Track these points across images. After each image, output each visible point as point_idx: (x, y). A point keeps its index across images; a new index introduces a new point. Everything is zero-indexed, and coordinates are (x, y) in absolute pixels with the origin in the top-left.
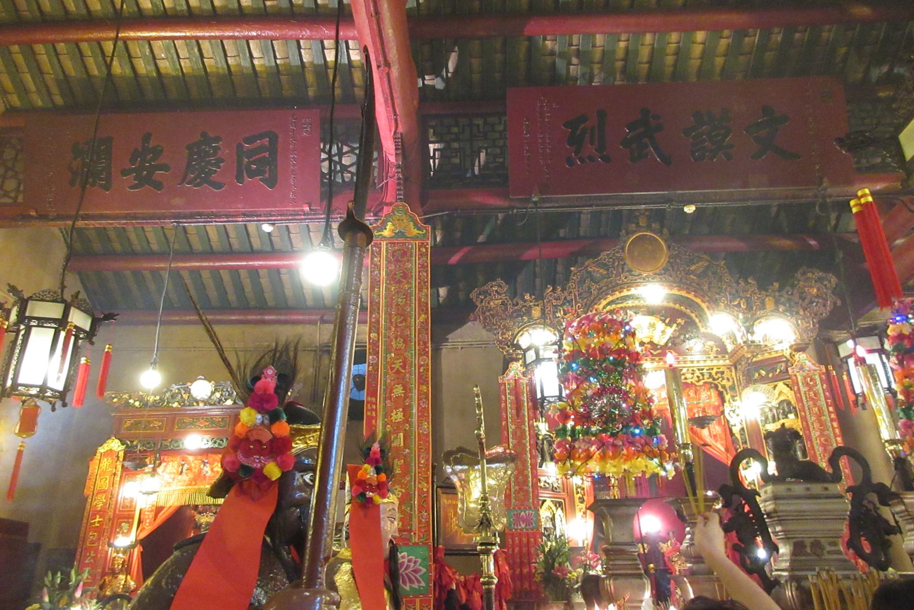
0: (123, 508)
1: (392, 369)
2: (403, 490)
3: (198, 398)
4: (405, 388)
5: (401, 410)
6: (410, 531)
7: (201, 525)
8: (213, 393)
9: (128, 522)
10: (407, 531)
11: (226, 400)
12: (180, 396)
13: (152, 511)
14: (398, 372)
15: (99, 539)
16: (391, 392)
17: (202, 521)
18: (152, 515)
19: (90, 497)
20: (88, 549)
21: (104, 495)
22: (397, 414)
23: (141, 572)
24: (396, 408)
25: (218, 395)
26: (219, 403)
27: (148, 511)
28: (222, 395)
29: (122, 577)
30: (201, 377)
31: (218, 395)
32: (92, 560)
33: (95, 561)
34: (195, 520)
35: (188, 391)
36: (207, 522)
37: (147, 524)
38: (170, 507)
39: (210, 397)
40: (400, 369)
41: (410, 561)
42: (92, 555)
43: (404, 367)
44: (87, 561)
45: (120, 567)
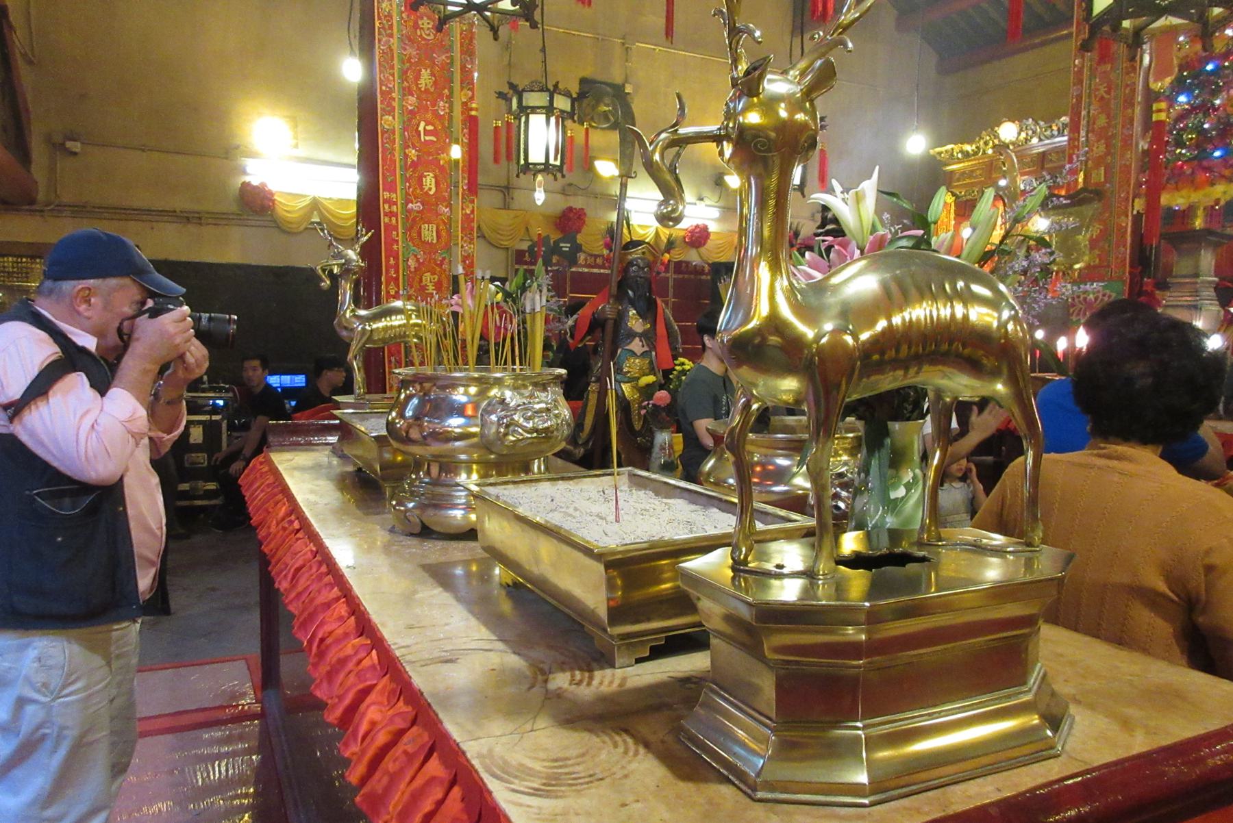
1: (1096, 96)
2: (1101, 227)
3: (1007, 141)
4: (1108, 116)
5: (1103, 141)
6: (1109, 266)
8: (1019, 134)
10: (1105, 267)
11: (1031, 138)
12: (991, 142)
14: (1102, 98)
16: (1094, 123)
22: (1098, 148)
24: (1098, 141)
25: (1023, 135)
26: (1026, 143)
28: (1027, 134)
30: (1004, 119)
31: (1023, 135)
35: (997, 136)
39: (1017, 138)
40: (1106, 96)
41: (1104, 295)
43: (1108, 92)
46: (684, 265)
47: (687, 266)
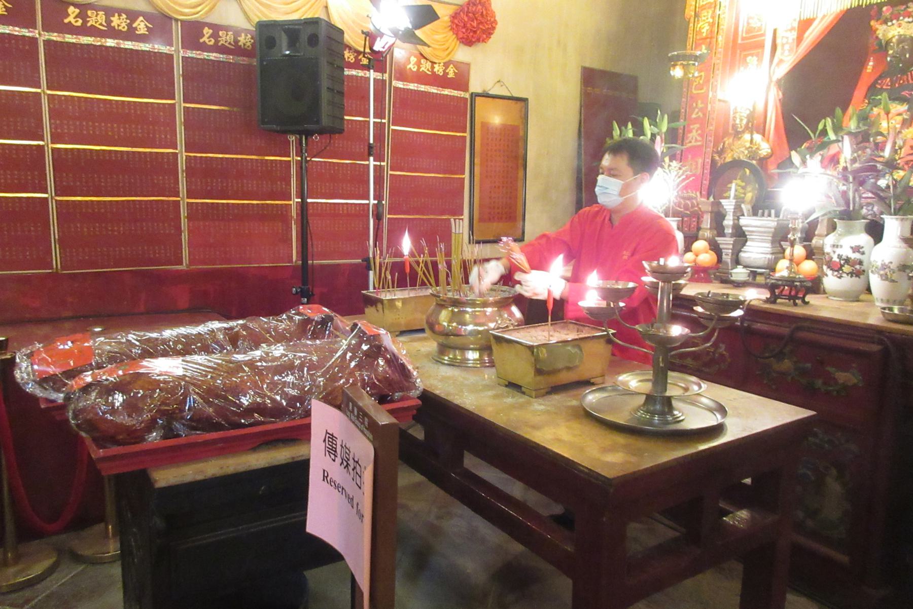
0: (747, 33)
7: (888, 42)
9: (757, 55)
13: (793, 29)
15: (708, 81)
17: (890, 35)
18: (794, 34)
19: (692, 20)
20: (693, 98)
21: (710, 12)
23: (782, 132)
27: (786, 31)
29: (747, 136)
32: (700, 114)
33: (704, 115)
34: (877, 37)
36: (900, 36)
37: (787, 53)
38: (824, 16)
42: (700, 105)
44: (694, 116)
45: (745, 122)
46: (207, 31)
47: (215, 35)
